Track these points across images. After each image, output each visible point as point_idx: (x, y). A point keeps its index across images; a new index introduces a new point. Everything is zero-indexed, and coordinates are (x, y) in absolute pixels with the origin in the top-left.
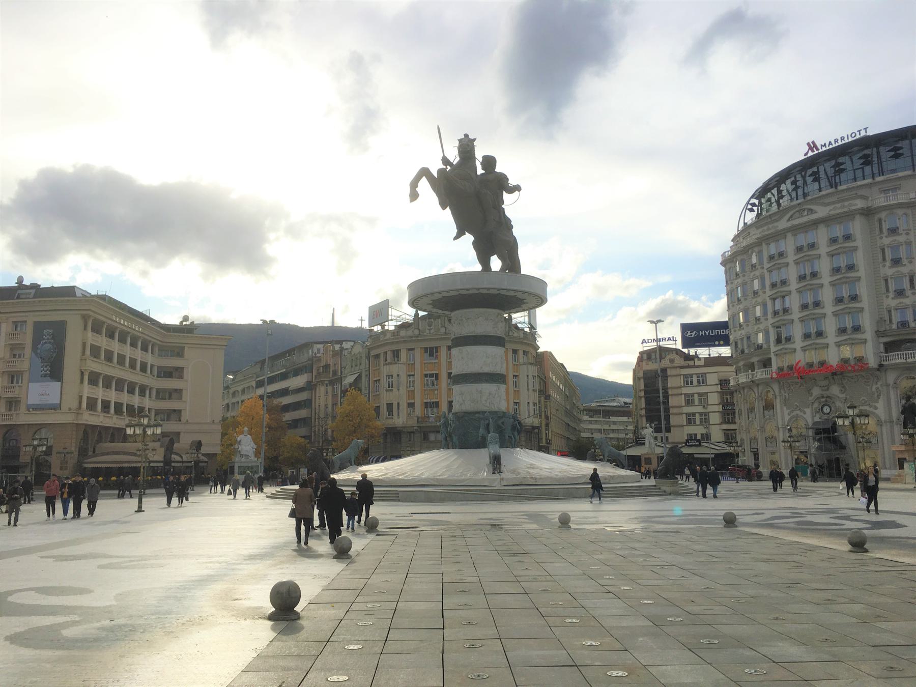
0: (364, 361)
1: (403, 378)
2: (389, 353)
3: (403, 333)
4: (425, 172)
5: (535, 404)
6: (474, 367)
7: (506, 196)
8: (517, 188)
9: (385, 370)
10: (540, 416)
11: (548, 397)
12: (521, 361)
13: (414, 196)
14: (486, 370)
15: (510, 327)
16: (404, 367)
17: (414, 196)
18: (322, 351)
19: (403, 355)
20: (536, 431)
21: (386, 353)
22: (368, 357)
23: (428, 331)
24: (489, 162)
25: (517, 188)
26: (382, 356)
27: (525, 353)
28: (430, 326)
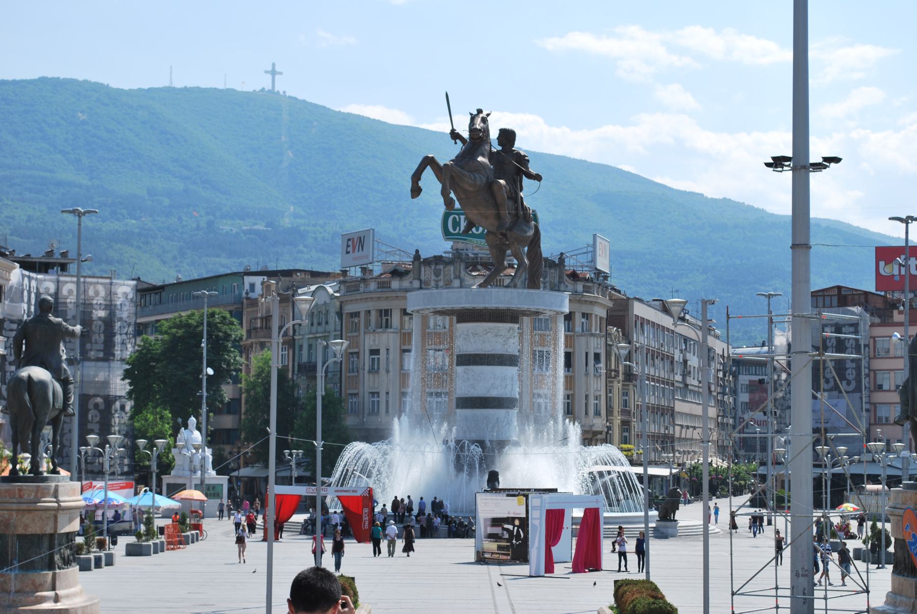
0: (333, 318)
1: (394, 354)
2: (373, 314)
3: (395, 284)
4: (428, 162)
5: (596, 398)
6: (480, 391)
7: (525, 180)
8: (538, 178)
9: (369, 342)
10: (609, 411)
11: (629, 376)
12: (578, 329)
13: (416, 191)
14: (494, 393)
15: (561, 277)
16: (397, 337)
17: (416, 191)
18: (258, 289)
19: (396, 319)
20: (599, 436)
21: (369, 312)
22: (340, 314)
23: (433, 284)
24: (507, 136)
25: (538, 178)
26: (362, 315)
27: (584, 315)
28: (437, 274)
